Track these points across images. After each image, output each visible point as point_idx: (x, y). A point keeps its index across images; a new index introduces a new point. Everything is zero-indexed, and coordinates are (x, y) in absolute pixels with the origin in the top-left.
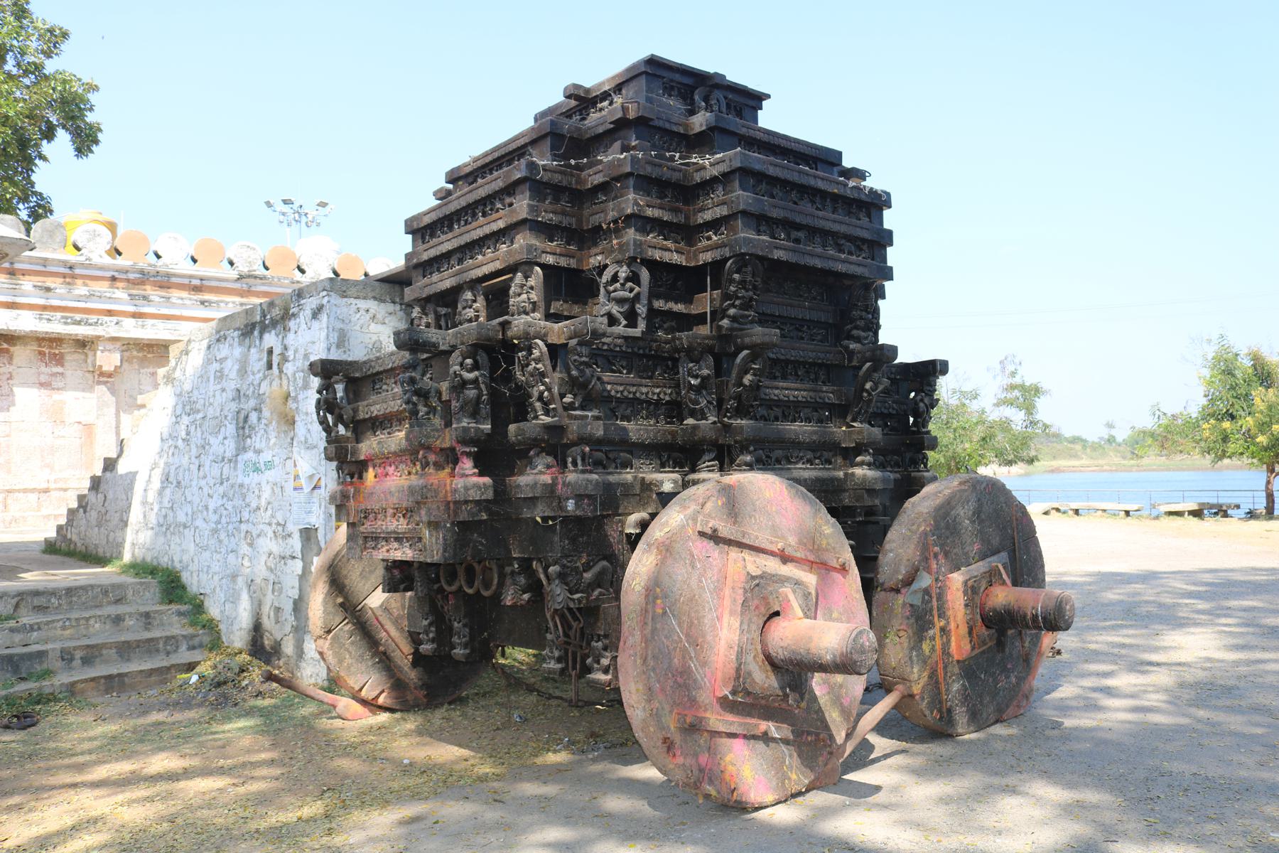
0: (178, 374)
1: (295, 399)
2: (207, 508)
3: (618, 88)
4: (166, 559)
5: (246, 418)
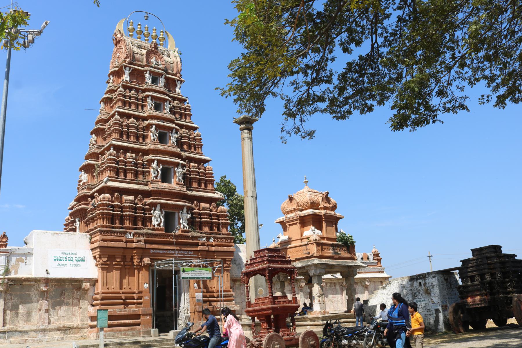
5: (415, 294)
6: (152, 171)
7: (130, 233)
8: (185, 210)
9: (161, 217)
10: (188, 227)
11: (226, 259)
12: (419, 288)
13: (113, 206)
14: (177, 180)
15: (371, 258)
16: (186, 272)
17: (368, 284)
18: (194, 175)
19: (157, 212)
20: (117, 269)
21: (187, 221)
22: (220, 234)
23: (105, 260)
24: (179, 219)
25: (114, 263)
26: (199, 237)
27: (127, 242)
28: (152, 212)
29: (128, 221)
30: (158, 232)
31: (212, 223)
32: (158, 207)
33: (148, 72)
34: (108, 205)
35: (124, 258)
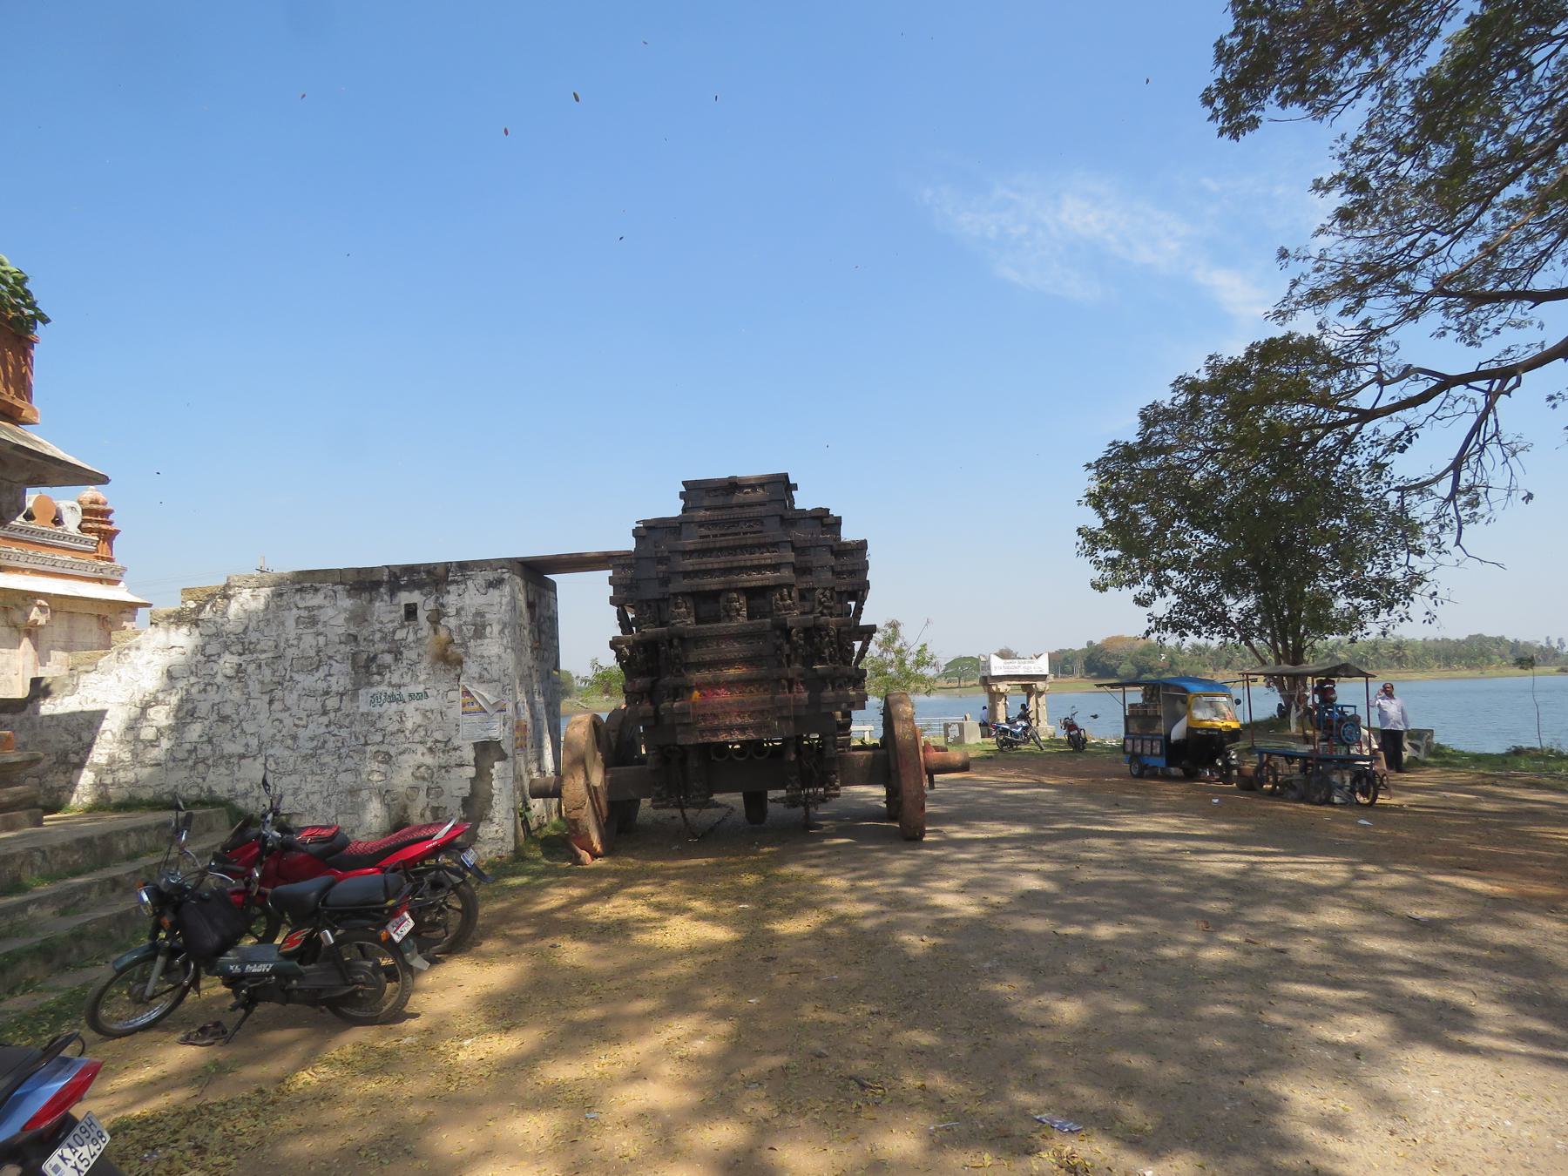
0: (207, 613)
1: (464, 644)
2: (294, 738)
3: (762, 485)
4: (194, 792)
12: (400, 635)
15: (72, 522)
17: (42, 620)
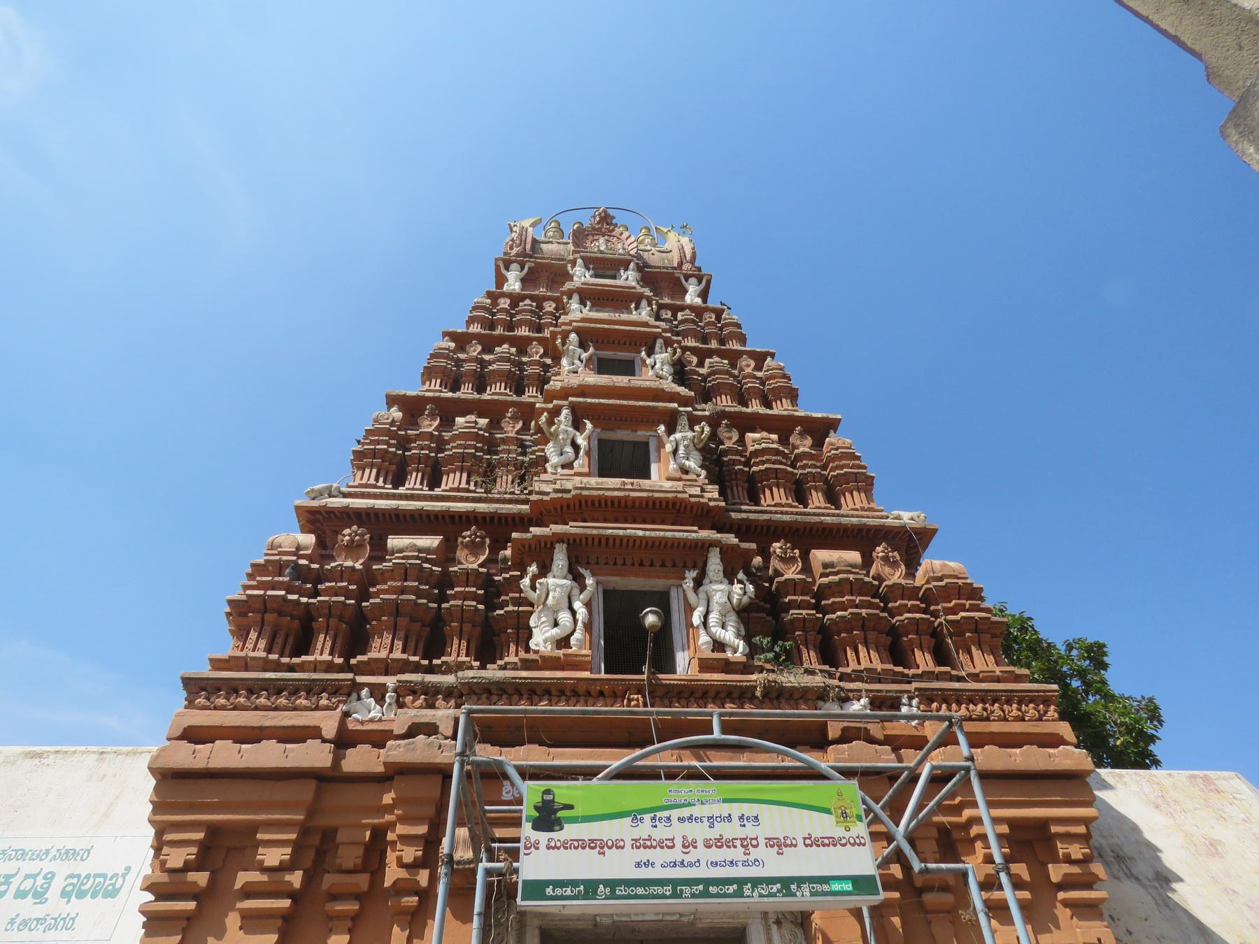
6: (550, 450)
7: (378, 693)
8: (715, 564)
9: (577, 605)
10: (741, 645)
11: (1044, 823)
13: (319, 577)
14: (673, 465)
16: (570, 831)
18: (763, 463)
19: (550, 581)
20: (252, 922)
21: (732, 620)
22: (960, 679)
23: (177, 858)
24: (690, 609)
25: (243, 878)
26: (821, 695)
27: (344, 740)
28: (526, 581)
29: (387, 638)
30: (547, 674)
31: (894, 633)
32: (560, 560)
33: (579, 261)
34: (279, 567)
35: (316, 847)
